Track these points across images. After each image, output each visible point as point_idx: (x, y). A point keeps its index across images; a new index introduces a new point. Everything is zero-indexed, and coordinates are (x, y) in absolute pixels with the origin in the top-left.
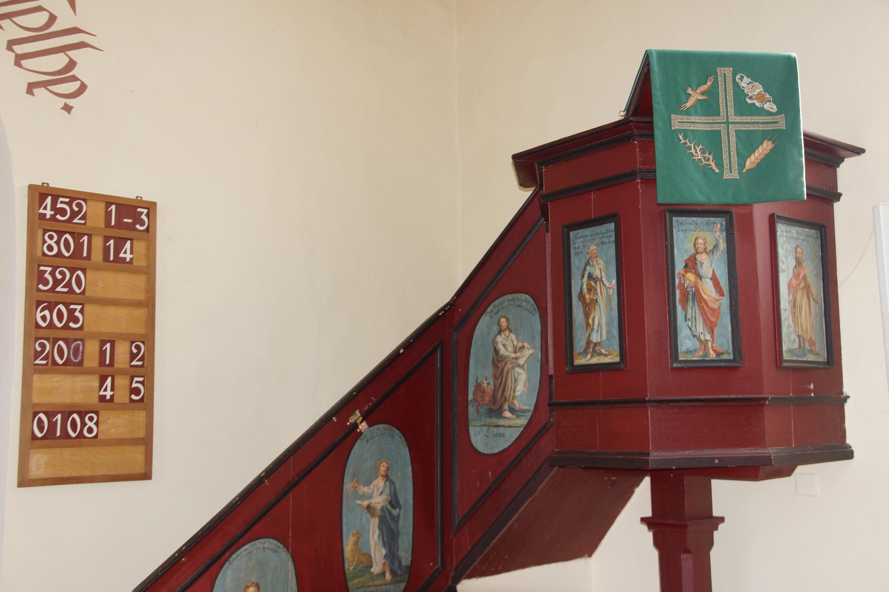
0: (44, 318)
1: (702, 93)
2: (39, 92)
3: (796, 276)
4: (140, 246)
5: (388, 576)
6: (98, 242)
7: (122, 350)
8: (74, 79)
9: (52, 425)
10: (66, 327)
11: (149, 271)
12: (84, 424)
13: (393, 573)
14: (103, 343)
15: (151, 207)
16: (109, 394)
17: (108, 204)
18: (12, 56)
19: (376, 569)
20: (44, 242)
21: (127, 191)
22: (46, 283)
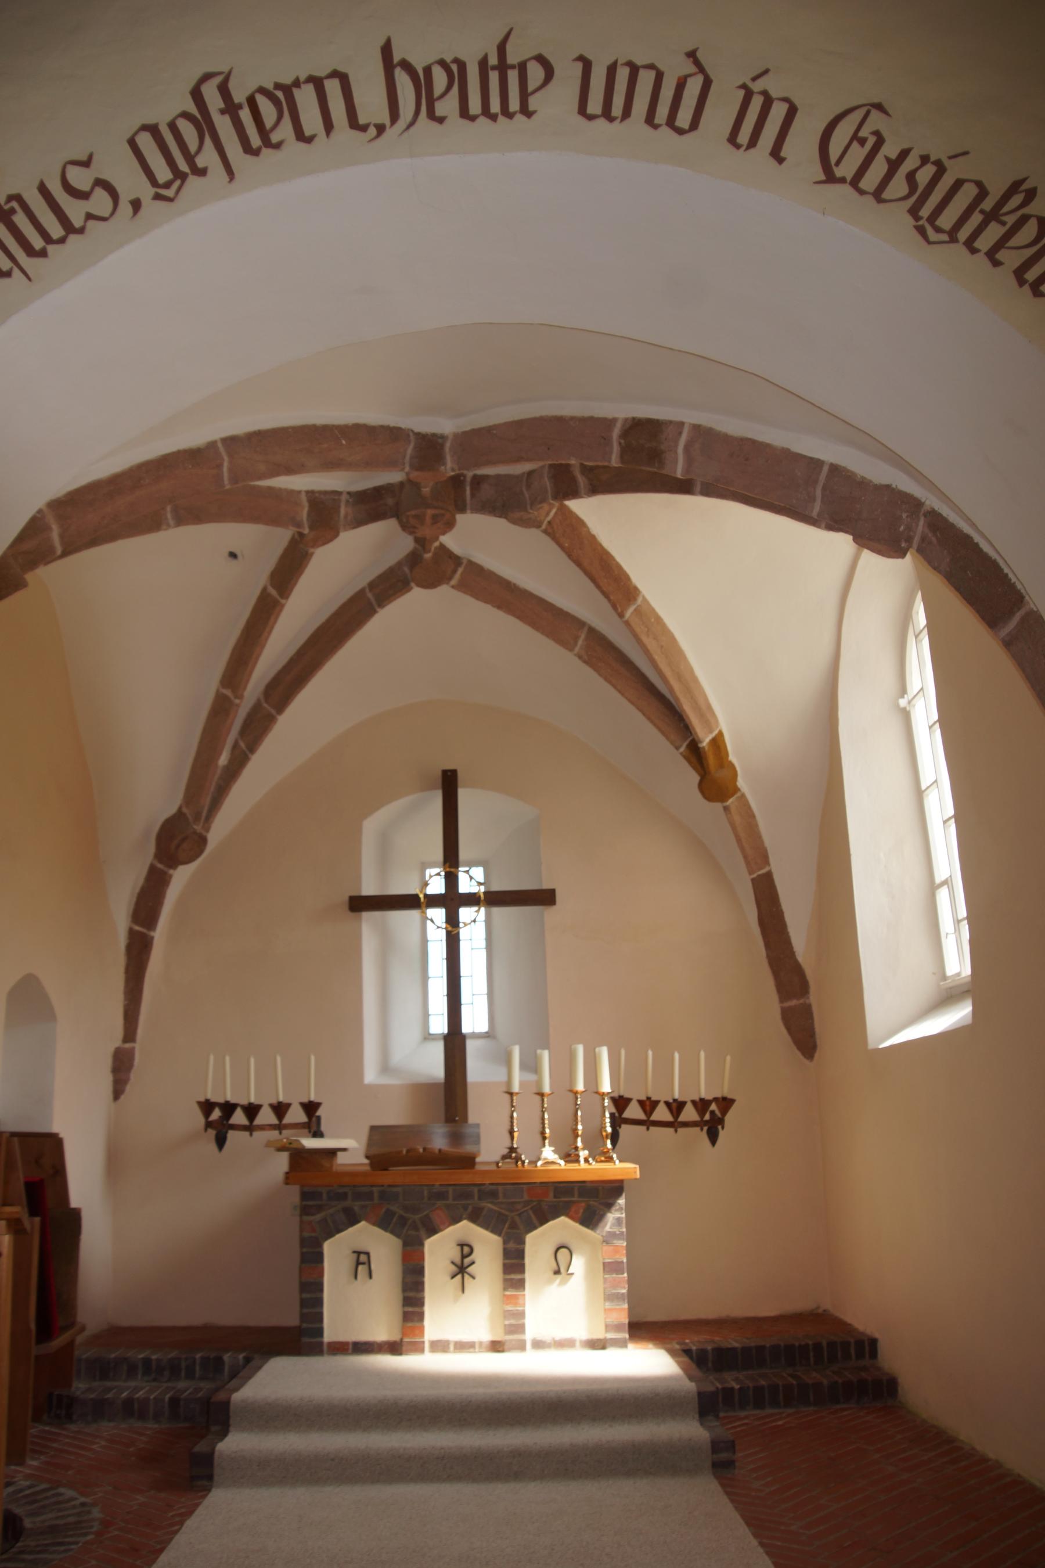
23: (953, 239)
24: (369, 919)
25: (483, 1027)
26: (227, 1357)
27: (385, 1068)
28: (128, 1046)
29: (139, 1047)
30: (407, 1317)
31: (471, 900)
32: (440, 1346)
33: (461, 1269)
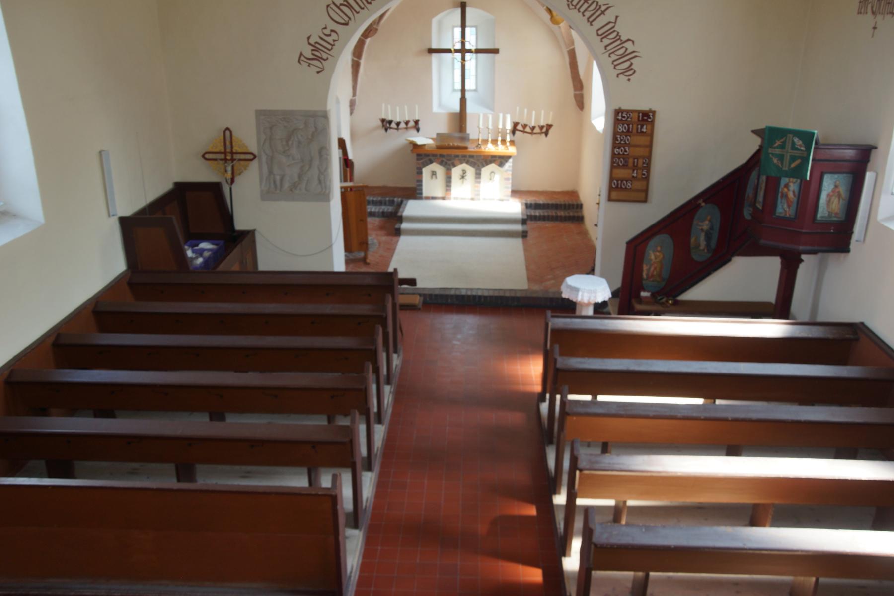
0: (617, 152)
1: (781, 142)
2: (621, 76)
3: (833, 191)
4: (649, 127)
5: (706, 251)
6: (635, 126)
7: (641, 161)
8: (632, 69)
9: (618, 184)
10: (624, 154)
11: (651, 135)
12: (627, 184)
13: (708, 250)
14: (634, 159)
15: (654, 113)
16: (635, 175)
17: (639, 113)
18: (613, 65)
19: (702, 248)
20: (618, 127)
21: (645, 107)
22: (618, 140)
23: (575, 8)
24: (435, 56)
25: (473, 87)
26: (396, 199)
27: (440, 105)
28: (354, 98)
29: (356, 98)
30: (447, 190)
31: (470, 51)
32: (456, 198)
33: (463, 177)
